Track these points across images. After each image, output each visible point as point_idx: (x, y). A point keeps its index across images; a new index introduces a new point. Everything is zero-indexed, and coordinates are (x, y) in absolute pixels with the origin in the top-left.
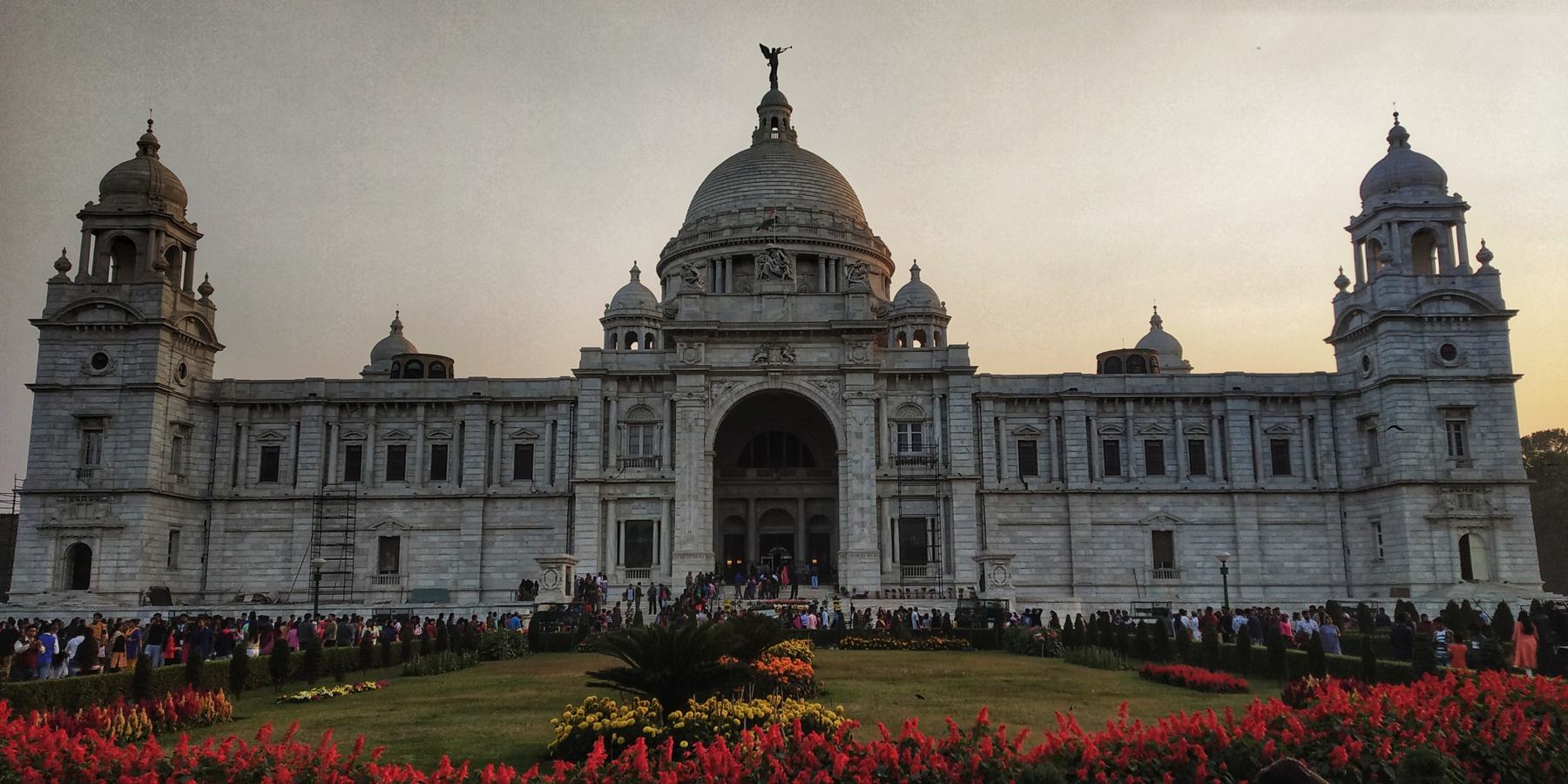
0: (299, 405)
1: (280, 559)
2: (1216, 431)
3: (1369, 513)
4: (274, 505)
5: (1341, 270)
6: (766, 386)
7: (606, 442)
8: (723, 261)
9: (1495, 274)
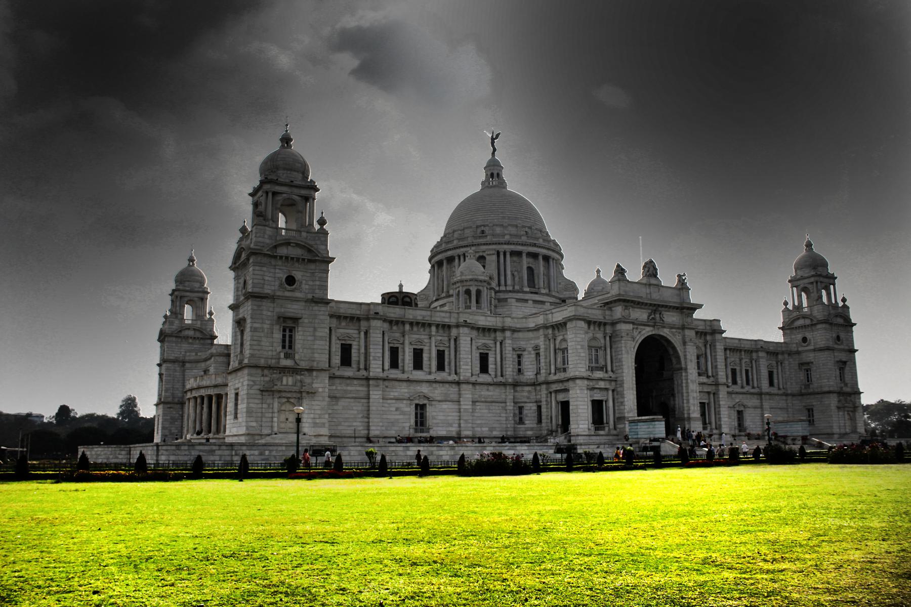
0: (368, 319)
1: (360, 416)
3: (804, 404)
4: (355, 382)
6: (654, 333)
8: (505, 253)
9: (848, 308)
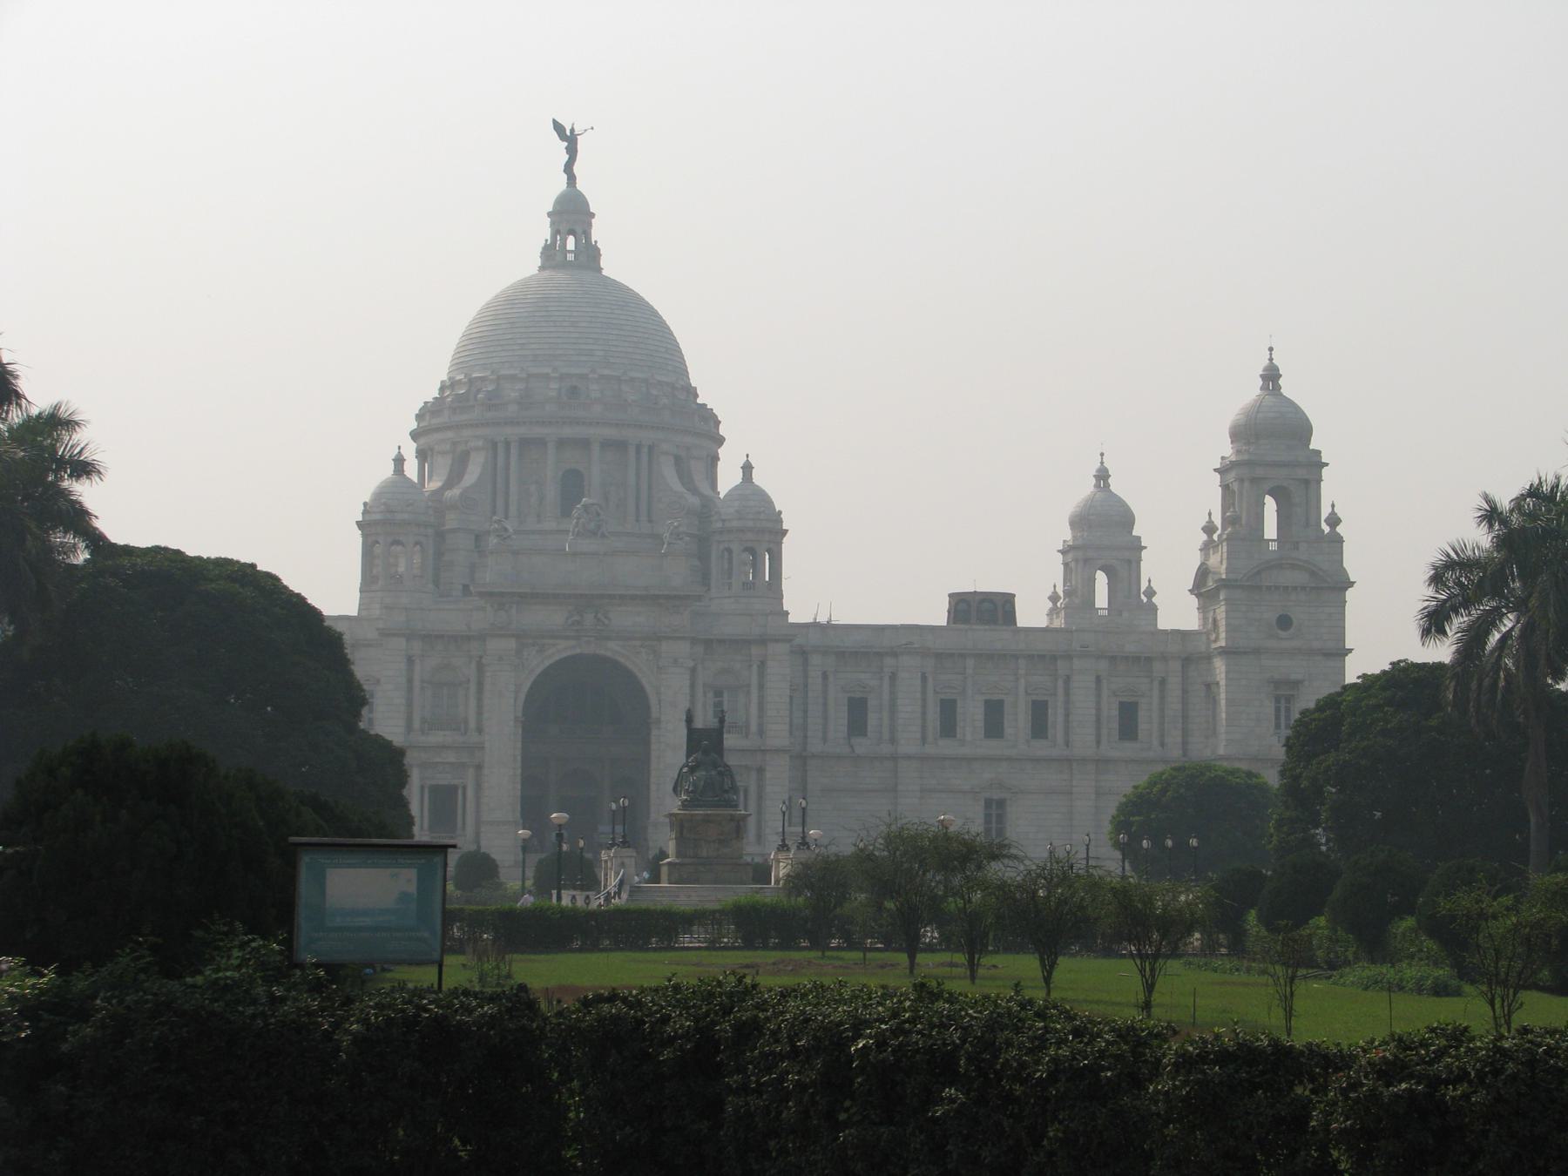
2: (1061, 691)
5: (1210, 514)
6: (578, 651)
7: (409, 703)
8: (507, 444)
9: (1338, 541)
